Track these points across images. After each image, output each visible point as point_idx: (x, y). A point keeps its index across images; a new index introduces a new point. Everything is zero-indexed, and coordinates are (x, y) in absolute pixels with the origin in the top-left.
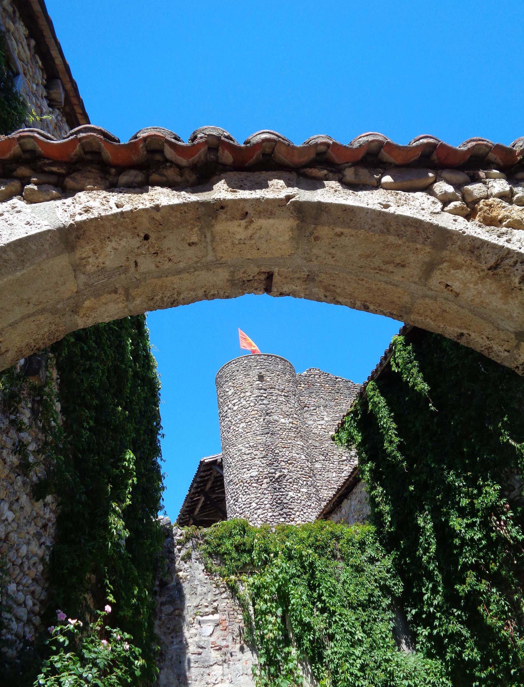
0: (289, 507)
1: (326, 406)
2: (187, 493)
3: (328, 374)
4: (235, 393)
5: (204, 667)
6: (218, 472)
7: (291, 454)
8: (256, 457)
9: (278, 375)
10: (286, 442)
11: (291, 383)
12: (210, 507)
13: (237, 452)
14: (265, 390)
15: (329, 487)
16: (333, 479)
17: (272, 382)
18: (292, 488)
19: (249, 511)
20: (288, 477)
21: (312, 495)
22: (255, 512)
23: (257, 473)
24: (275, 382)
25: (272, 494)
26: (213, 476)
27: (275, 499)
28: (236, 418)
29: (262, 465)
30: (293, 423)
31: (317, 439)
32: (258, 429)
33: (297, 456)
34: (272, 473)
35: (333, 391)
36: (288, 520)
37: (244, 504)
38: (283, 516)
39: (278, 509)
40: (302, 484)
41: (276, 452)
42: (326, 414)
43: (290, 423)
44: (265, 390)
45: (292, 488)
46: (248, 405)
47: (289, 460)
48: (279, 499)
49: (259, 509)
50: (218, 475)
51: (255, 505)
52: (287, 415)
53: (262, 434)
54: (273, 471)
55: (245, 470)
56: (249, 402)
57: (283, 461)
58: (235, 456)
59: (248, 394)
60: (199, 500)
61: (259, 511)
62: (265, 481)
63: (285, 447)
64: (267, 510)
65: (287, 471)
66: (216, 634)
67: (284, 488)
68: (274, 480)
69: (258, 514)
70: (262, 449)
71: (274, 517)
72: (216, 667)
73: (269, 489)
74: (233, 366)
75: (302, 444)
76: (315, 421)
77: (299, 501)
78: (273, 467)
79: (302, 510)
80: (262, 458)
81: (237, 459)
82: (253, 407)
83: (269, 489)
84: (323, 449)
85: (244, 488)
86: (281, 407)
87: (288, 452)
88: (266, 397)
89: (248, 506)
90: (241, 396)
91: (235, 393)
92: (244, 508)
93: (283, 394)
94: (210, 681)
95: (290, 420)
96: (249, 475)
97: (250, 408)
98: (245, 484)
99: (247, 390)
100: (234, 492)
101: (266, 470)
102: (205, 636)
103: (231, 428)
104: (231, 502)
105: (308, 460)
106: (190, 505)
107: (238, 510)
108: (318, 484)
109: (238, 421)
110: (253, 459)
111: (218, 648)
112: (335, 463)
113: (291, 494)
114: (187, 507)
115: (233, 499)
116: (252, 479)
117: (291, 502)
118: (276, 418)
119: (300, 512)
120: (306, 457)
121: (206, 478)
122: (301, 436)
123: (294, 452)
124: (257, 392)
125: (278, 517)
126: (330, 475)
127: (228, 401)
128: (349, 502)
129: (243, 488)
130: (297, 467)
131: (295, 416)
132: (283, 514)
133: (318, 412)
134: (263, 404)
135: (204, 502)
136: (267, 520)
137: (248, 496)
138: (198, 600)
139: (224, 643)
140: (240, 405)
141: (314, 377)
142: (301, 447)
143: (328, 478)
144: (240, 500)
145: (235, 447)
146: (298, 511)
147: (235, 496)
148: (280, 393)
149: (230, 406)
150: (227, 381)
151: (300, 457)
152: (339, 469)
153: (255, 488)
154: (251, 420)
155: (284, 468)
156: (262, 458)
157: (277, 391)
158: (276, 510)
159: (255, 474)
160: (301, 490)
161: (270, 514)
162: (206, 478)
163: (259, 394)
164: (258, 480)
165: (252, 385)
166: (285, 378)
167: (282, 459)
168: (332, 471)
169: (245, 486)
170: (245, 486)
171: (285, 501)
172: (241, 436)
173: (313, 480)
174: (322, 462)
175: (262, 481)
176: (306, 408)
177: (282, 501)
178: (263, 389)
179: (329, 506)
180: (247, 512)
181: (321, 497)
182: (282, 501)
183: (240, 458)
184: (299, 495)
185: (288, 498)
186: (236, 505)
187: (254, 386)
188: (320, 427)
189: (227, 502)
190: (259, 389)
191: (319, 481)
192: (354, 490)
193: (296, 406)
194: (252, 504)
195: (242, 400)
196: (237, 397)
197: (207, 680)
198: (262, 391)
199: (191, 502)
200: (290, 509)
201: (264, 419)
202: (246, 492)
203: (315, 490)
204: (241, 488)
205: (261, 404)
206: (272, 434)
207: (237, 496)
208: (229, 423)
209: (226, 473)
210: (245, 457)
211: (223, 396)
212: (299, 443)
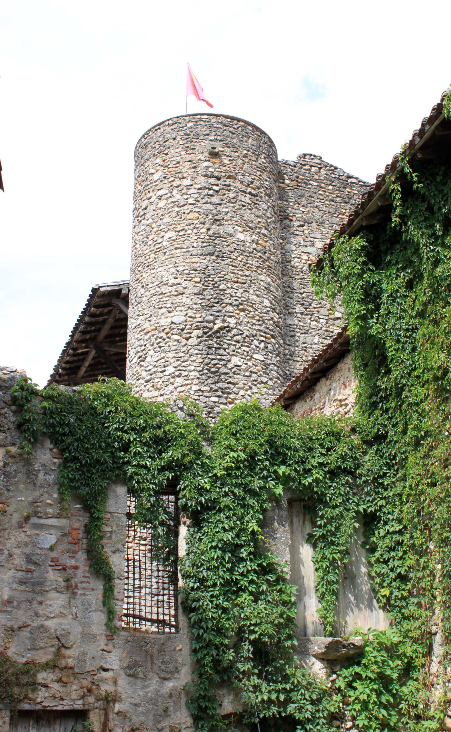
0: (230, 380)
1: (323, 223)
2: (67, 339)
3: (336, 168)
4: (165, 178)
5: (34, 592)
6: (121, 312)
7: (246, 295)
8: (185, 291)
9: (245, 156)
10: (240, 273)
11: (265, 173)
12: (106, 368)
13: (154, 280)
14: (219, 179)
15: (304, 358)
16: (314, 346)
17: (232, 166)
18: (239, 351)
19: (161, 378)
20: (234, 332)
21: (272, 367)
22: (171, 380)
23: (183, 318)
24: (237, 168)
25: (204, 356)
26: (112, 315)
27: (207, 364)
28: (160, 222)
29: (195, 306)
30: (257, 244)
31: (297, 277)
32: (195, 245)
33: (258, 300)
34: (209, 322)
35: (338, 199)
36: (224, 401)
37: (155, 366)
38: (217, 393)
39: (210, 381)
40: (257, 347)
41: (221, 287)
42: (319, 235)
43: (253, 241)
44: (219, 179)
45: (239, 351)
47: (241, 304)
48: (215, 365)
49: (179, 376)
50: (122, 316)
51: (173, 370)
52: (250, 228)
53: (202, 254)
54: (212, 318)
55: (163, 310)
56: (186, 197)
57: (231, 304)
58: (151, 286)
59: (187, 182)
60: (86, 353)
61: (178, 379)
62: (196, 333)
63: (237, 282)
64: (193, 379)
65: (235, 321)
66: (60, 548)
67: (225, 349)
68: (210, 333)
69: (176, 385)
70: (198, 280)
71: (200, 393)
72: (53, 594)
73: (200, 347)
74: (167, 128)
75: (269, 280)
76: (298, 245)
77: (247, 374)
78: (211, 312)
79: (251, 388)
80: (196, 294)
81: (153, 292)
82: (191, 207)
83: (200, 347)
84: (304, 295)
85: (159, 340)
86: (242, 212)
87: (241, 291)
88: (217, 192)
89: (160, 370)
90: (175, 184)
91: (165, 178)
92: (155, 372)
93: (249, 190)
94: (41, 612)
95: (254, 237)
96: (169, 320)
97: (186, 207)
98: (162, 334)
99: (185, 175)
100: (141, 346)
101: (198, 315)
102: (41, 549)
103: (150, 238)
104: (134, 361)
105: (274, 309)
106: (72, 359)
107: (144, 374)
108: (287, 352)
109: (162, 227)
110: (180, 294)
111: (61, 568)
112: (321, 321)
113: (236, 360)
114: (67, 362)
115: (138, 355)
116: (173, 326)
117: (234, 373)
118: (229, 229)
119: (247, 390)
120: (271, 303)
121: (101, 319)
122: (269, 266)
123: (252, 292)
124: (202, 181)
125: (209, 394)
126: (309, 339)
127: (151, 190)
128: (328, 382)
129: (156, 340)
130: (253, 317)
131: (264, 231)
132: (216, 391)
133: (306, 232)
134: (210, 203)
135: (94, 358)
137: (163, 355)
138: (38, 493)
139: (73, 562)
140: (170, 200)
141: (310, 170)
142: (266, 285)
143: (304, 343)
144: (148, 359)
145: (153, 271)
146: (243, 388)
147: (142, 351)
148: (244, 188)
149: (151, 200)
150: (154, 155)
151: (261, 303)
152: (326, 331)
153: (176, 343)
154: (186, 228)
155: (231, 317)
156: (196, 294)
157: (238, 184)
158: (206, 382)
159: (179, 317)
160: (255, 356)
161: (195, 388)
162: (101, 319)
163: (206, 185)
164: (183, 330)
165: (195, 167)
166: (257, 164)
167: (230, 302)
168: (314, 333)
169: (161, 338)
170: (161, 338)
171: (223, 370)
172: (165, 253)
173: (278, 343)
174: (300, 316)
175: (191, 333)
176: (287, 222)
177: (219, 368)
178: (216, 177)
179: (294, 387)
180: (157, 380)
181: (288, 372)
182: (219, 368)
183: (158, 289)
184: (250, 364)
185: (230, 365)
186: (141, 366)
187: (199, 169)
188: (305, 257)
189: (128, 360)
190: (206, 176)
191: (287, 347)
192: (340, 366)
193: (268, 215)
195: (175, 192)
196: (167, 185)
197: (36, 610)
198: (212, 180)
199: (74, 355)
200: (229, 383)
201: (209, 229)
202: (160, 347)
203: (278, 359)
204: (153, 339)
205: (206, 203)
206: (218, 256)
207: (144, 352)
208: (148, 229)
209: (131, 311)
210: (165, 289)
211: (143, 181)
212: (262, 277)
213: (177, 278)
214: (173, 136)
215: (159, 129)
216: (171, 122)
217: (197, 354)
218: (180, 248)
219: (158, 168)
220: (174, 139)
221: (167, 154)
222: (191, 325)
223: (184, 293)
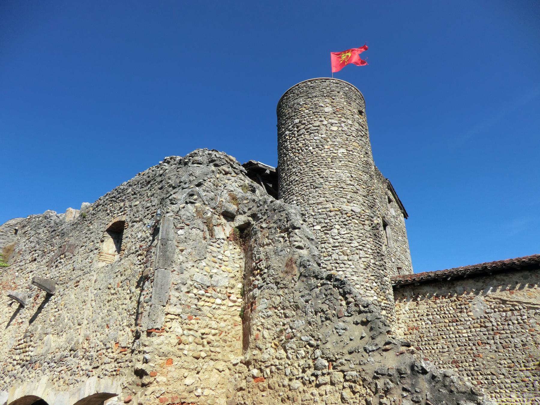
28: (334, 140)
46: (349, 134)
59: (350, 122)
92: (342, 242)
136: (369, 266)
172: (341, 161)
194: (353, 242)
213: (352, 181)
214: (338, 90)
215: (325, 82)
216: (334, 81)
217: (370, 237)
218: (351, 162)
219: (327, 105)
220: (338, 92)
221: (333, 99)
222: (364, 216)
223: (357, 193)
